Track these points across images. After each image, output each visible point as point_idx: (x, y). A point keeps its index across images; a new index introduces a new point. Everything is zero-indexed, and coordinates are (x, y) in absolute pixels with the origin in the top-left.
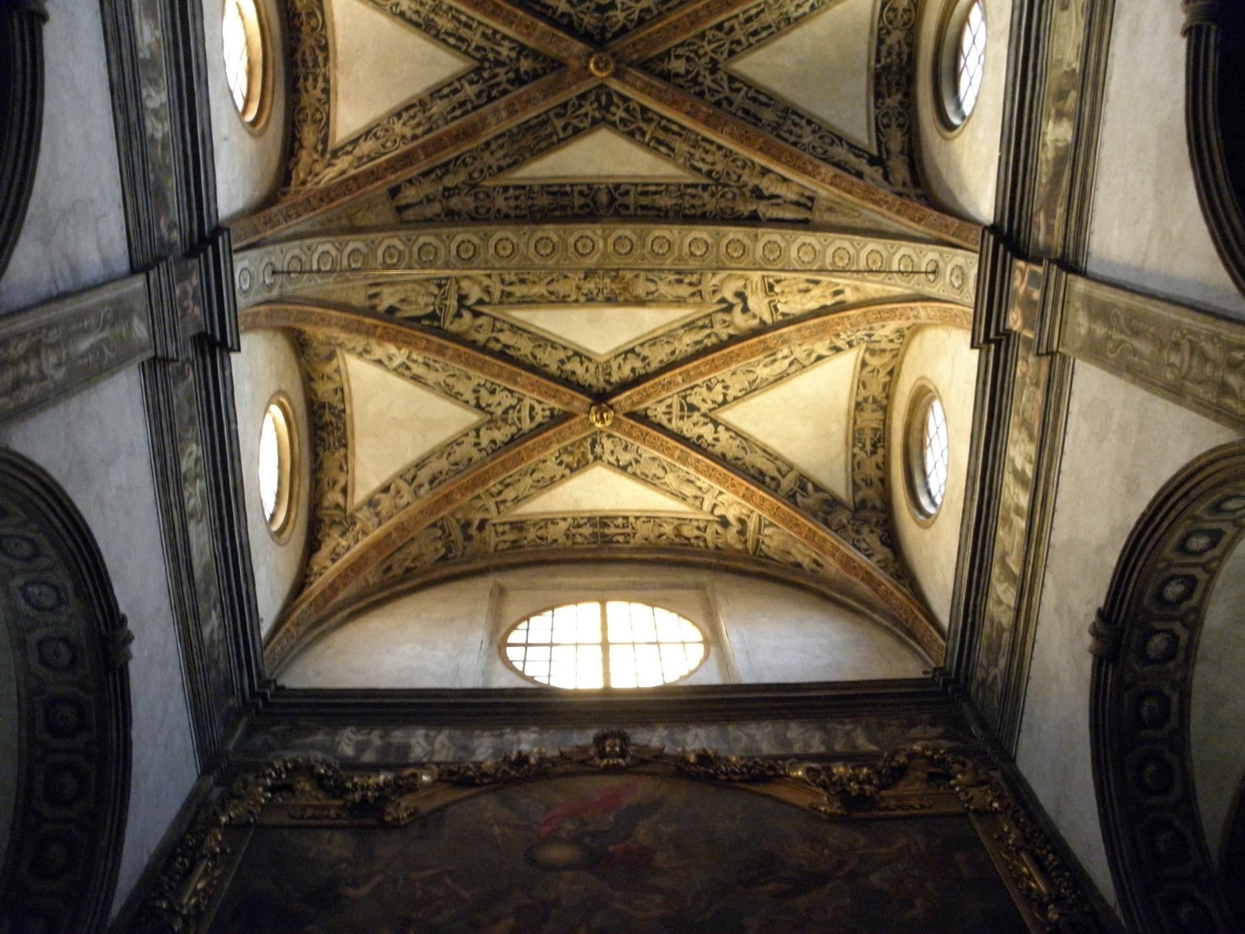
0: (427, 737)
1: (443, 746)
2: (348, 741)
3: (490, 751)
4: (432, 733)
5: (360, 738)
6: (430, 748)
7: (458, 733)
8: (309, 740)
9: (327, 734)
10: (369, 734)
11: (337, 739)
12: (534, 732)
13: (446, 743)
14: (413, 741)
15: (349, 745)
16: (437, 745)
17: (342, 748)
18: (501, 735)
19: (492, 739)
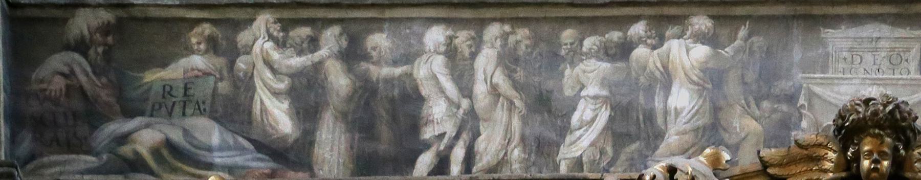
0: (451, 53)
1: (494, 91)
2: (268, 74)
3: (604, 116)
4: (463, 37)
5: (297, 62)
6: (465, 103)
7: (522, 33)
8: (175, 72)
9: (213, 45)
10: (314, 43)
11: (241, 64)
12: (701, 38)
13: (500, 78)
14: (421, 71)
15: (276, 94)
16: (480, 89)
17: (264, 110)
18: (624, 50)
19: (605, 66)
